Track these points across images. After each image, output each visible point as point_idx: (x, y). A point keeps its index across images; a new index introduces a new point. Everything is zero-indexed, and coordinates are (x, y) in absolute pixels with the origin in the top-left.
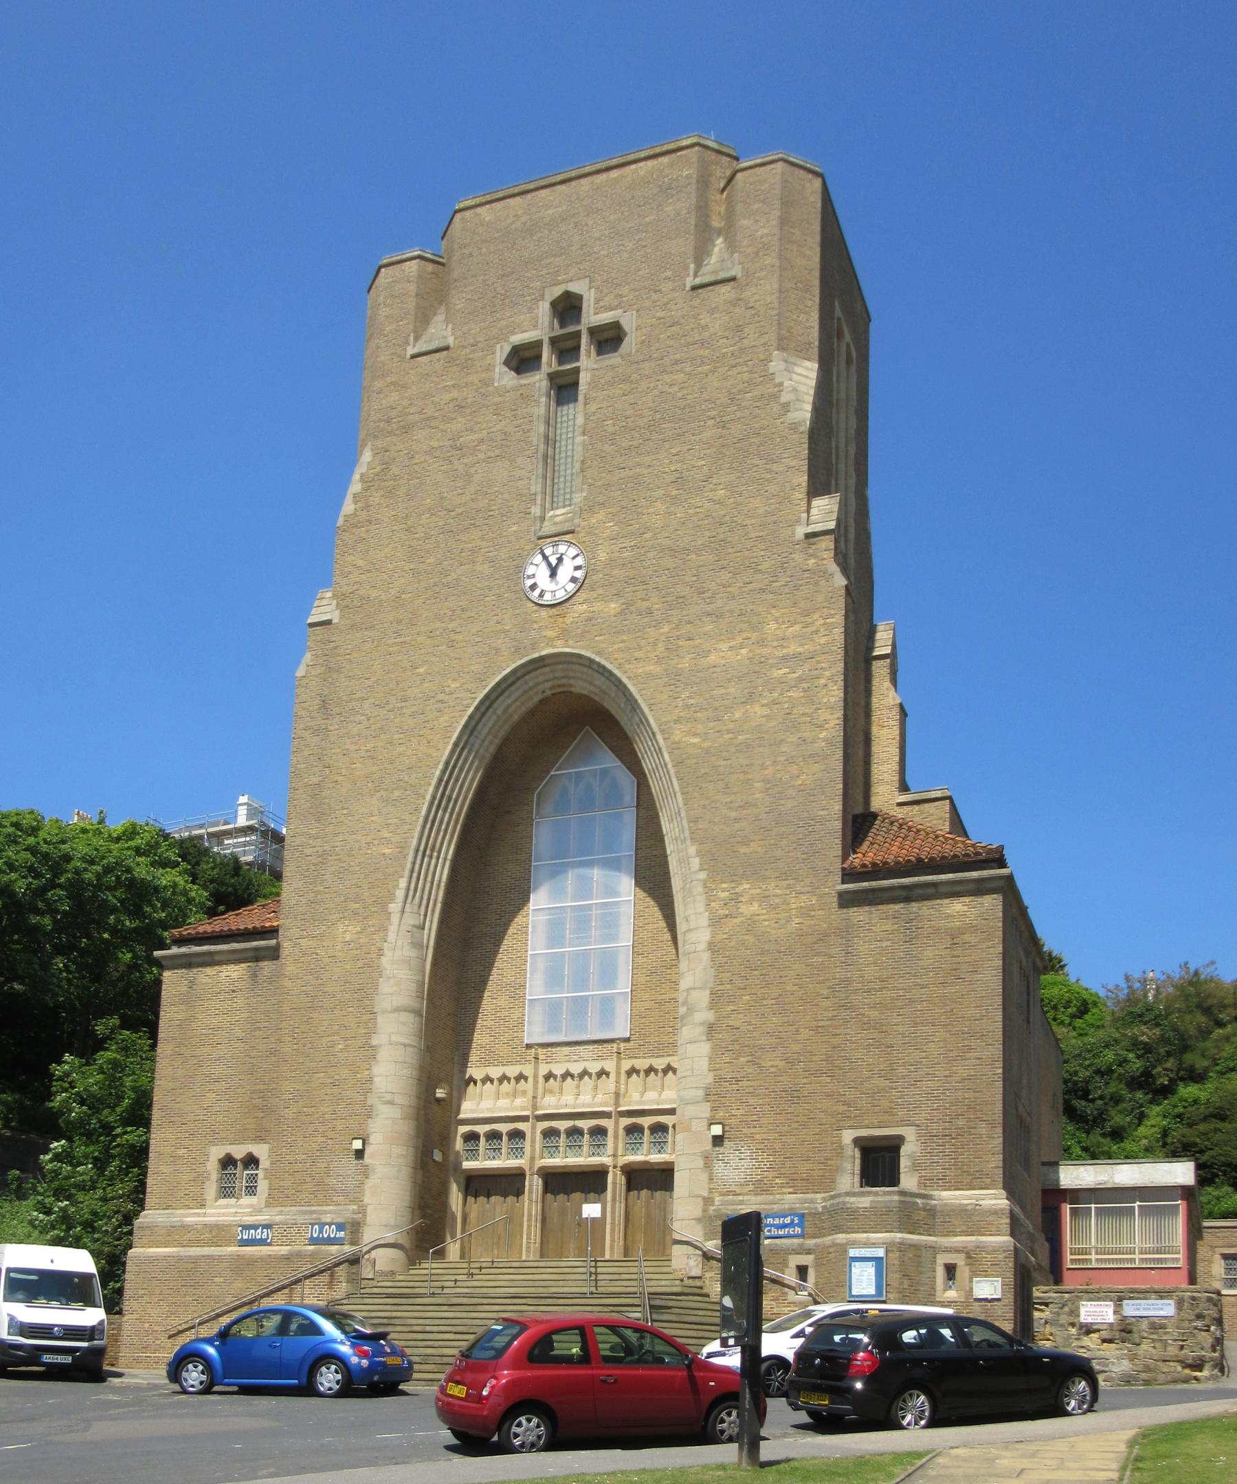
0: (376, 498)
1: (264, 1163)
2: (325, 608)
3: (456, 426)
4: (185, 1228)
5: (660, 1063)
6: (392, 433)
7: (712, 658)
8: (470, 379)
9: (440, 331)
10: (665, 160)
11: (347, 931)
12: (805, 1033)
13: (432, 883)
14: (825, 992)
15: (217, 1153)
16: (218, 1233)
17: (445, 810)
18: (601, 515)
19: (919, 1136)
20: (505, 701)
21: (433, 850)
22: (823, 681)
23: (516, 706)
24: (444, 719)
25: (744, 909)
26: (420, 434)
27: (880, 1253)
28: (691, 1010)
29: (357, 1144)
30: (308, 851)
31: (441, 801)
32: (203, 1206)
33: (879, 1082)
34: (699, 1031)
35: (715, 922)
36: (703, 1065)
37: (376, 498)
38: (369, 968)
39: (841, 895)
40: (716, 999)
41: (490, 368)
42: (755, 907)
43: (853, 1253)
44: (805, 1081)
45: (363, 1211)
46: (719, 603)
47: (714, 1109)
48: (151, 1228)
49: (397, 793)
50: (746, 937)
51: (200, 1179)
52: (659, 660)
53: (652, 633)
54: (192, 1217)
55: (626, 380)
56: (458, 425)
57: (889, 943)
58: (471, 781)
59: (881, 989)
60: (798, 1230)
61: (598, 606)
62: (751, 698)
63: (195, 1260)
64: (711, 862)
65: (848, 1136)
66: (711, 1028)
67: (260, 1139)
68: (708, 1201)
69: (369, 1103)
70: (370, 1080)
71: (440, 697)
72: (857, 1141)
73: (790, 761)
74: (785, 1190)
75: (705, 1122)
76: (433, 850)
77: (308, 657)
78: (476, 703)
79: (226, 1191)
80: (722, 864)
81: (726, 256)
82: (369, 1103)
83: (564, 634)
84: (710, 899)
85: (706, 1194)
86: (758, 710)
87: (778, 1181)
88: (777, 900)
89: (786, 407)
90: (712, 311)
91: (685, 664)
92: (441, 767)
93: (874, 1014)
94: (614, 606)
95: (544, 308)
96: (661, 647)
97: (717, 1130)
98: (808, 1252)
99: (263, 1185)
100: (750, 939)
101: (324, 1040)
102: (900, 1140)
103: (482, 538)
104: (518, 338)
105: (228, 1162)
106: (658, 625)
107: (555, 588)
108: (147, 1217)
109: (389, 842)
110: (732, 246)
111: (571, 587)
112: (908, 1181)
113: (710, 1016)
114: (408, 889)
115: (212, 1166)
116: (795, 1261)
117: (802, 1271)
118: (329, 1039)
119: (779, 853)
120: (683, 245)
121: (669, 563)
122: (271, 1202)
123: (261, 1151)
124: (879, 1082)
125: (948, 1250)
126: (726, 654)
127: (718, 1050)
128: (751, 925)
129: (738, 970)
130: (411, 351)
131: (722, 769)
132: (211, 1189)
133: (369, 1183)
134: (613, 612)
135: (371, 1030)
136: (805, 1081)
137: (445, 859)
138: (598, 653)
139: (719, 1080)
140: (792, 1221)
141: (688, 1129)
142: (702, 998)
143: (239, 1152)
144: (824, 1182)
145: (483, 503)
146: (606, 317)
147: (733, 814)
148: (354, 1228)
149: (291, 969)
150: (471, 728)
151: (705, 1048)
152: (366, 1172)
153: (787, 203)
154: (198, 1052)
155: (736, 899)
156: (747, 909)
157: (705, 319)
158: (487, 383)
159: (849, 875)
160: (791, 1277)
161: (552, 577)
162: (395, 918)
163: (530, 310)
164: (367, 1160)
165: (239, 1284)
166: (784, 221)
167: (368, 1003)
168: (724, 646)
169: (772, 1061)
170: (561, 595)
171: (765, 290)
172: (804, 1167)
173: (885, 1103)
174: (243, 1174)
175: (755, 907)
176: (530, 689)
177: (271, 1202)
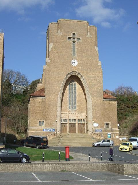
0: (54, 49)
3: (63, 44)
4: (36, 129)
6: (55, 43)
9: (60, 33)
10: (84, 23)
11: (53, 97)
16: (40, 130)
18: (79, 58)
23: (69, 75)
27: (110, 134)
28: (90, 110)
29: (56, 121)
32: (37, 126)
34: (91, 112)
35: (92, 101)
36: (92, 115)
37: (54, 49)
41: (66, 39)
43: (108, 134)
51: (37, 123)
53: (85, 71)
54: (36, 128)
55: (81, 44)
61: (79, 67)
63: (38, 133)
64: (91, 95)
65: (105, 123)
66: (92, 112)
67: (44, 119)
68: (93, 128)
70: (57, 114)
73: (98, 87)
79: (40, 125)
80: (93, 95)
81: (90, 34)
83: (76, 69)
84: (91, 98)
86: (95, 81)
89: (96, 52)
90: (89, 40)
95: (72, 34)
96: (86, 73)
97: (94, 121)
106: (85, 71)
107: (75, 65)
109: (58, 88)
110: (91, 33)
111: (77, 65)
116: (101, 134)
120: (86, 32)
121: (86, 64)
123: (44, 121)
125: (114, 133)
126: (92, 75)
127: (93, 114)
130: (57, 34)
132: (38, 124)
133: (57, 125)
135: (57, 108)
141: (90, 121)
142: (91, 108)
143: (41, 121)
144: (103, 127)
146: (78, 37)
148: (56, 130)
152: (57, 124)
153: (95, 31)
156: (96, 100)
157: (88, 41)
158: (66, 40)
159: (104, 99)
160: (101, 135)
161: (75, 63)
162: (59, 96)
163: (71, 34)
166: (95, 33)
168: (92, 74)
169: (98, 115)
170: (75, 65)
171: (94, 39)
174: (42, 123)
177: (46, 126)
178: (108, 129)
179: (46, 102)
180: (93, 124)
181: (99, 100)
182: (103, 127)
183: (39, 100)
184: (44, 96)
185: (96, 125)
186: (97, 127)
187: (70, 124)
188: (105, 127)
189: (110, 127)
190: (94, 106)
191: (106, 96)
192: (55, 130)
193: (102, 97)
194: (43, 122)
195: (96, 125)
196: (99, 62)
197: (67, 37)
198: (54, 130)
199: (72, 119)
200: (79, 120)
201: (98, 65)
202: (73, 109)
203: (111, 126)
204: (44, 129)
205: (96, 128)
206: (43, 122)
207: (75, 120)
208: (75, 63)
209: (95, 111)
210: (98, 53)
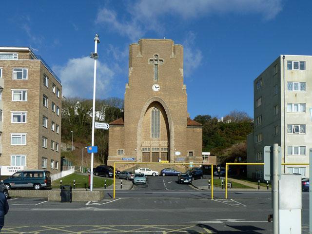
2: (127, 87)
3: (143, 67)
11: (133, 125)
15: (117, 150)
16: (119, 159)
35: (175, 129)
36: (174, 144)
40: (175, 137)
54: (115, 157)
62: (178, 106)
65: (188, 151)
66: (174, 140)
70: (136, 143)
83: (157, 95)
94: (163, 93)
104: (151, 59)
105: (119, 151)
107: (157, 90)
112: (194, 155)
122: (126, 155)
123: (124, 150)
126: (175, 100)
128: (178, 130)
151: (174, 142)
152: (137, 152)
177: (126, 155)
178: (190, 158)
180: (174, 153)
181: (182, 128)
184: (123, 125)
185: (178, 153)
186: (180, 156)
187: (153, 152)
188: (188, 156)
190: (177, 133)
191: (191, 123)
193: (186, 123)
195: (178, 153)
196: (184, 85)
197: (149, 60)
199: (145, 147)
200: (162, 149)
201: (183, 89)
202: (156, 137)
204: (123, 158)
205: (178, 156)
206: (122, 151)
207: (149, 148)
208: (156, 88)
210: (182, 75)
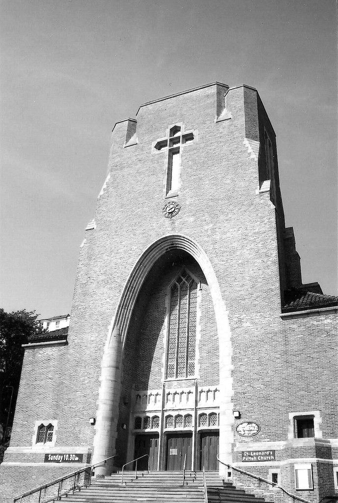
0: (111, 189)
1: (56, 428)
4: (24, 455)
5: (213, 388)
7: (228, 234)
8: (143, 152)
12: (271, 373)
13: (125, 318)
14: (278, 356)
15: (38, 423)
16: (34, 457)
17: (131, 292)
19: (321, 415)
20: (153, 253)
21: (126, 306)
22: (270, 241)
23: (157, 255)
24: (131, 260)
25: (245, 325)
26: (126, 170)
30: (79, 308)
31: (128, 288)
33: (303, 393)
35: (233, 330)
37: (111, 189)
38: (100, 350)
39: (282, 317)
40: (234, 359)
42: (248, 324)
44: (272, 393)
45: (93, 448)
46: (230, 216)
47: (235, 405)
48: (11, 454)
49: (113, 286)
50: (245, 335)
51: (32, 433)
52: (208, 236)
53: (206, 227)
54: (26, 450)
56: (139, 165)
57: (302, 336)
58: (142, 281)
59: (300, 354)
60: (272, 457)
65: (291, 416)
68: (234, 445)
69: (97, 404)
70: (98, 395)
71: (130, 252)
72: (295, 418)
74: (265, 440)
75: (232, 412)
76: (126, 306)
77: (85, 241)
78: (143, 253)
82: (97, 404)
85: (233, 442)
87: (263, 436)
88: (256, 320)
91: (217, 237)
92: (129, 276)
93: (298, 364)
94: (192, 219)
96: (209, 232)
97: (237, 414)
98: (277, 467)
99: (54, 437)
100: (247, 336)
101: (82, 379)
102: (313, 416)
103: (146, 200)
106: (208, 224)
108: (10, 450)
113: (232, 367)
114: (116, 320)
115: (36, 429)
117: (275, 476)
118: (83, 378)
119: (256, 303)
121: (211, 204)
123: (55, 423)
124: (303, 393)
129: (241, 349)
131: (233, 273)
132: (35, 437)
134: (192, 221)
136: (272, 393)
137: (130, 310)
138: (187, 235)
139: (236, 393)
140: (270, 454)
141: (224, 413)
143: (46, 424)
145: (146, 188)
147: (238, 289)
148: (89, 456)
149: (71, 351)
150: (140, 262)
151: (231, 380)
152: (94, 432)
154: (34, 383)
155: (240, 321)
164: (95, 427)
165: (42, 479)
167: (99, 364)
172: (273, 429)
173: (305, 401)
175: (248, 324)
176: (162, 248)
179: (69, 357)
182: (283, 436)
183: (50, 352)
189: (318, 433)
192: (85, 459)
194: (50, 427)
198: (80, 456)
203: (321, 428)
204: (47, 456)
209: (243, 369)
